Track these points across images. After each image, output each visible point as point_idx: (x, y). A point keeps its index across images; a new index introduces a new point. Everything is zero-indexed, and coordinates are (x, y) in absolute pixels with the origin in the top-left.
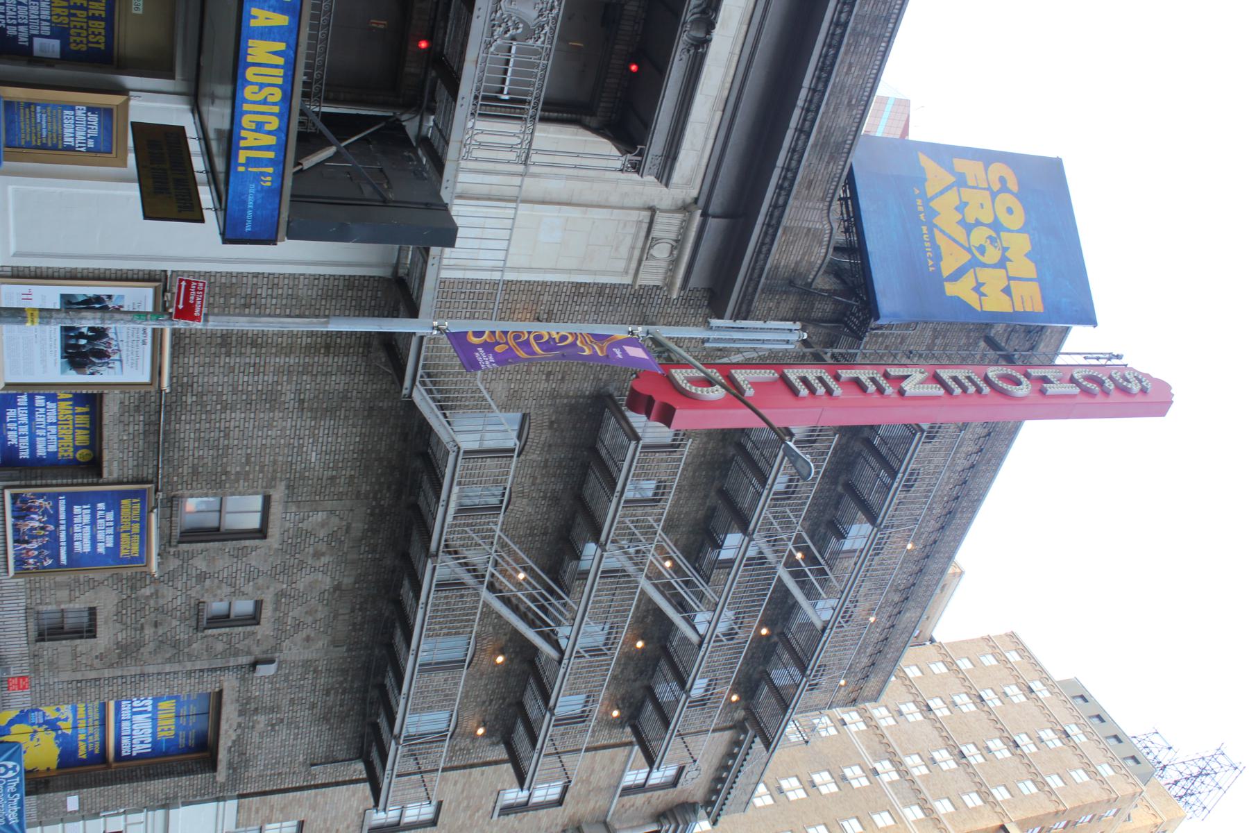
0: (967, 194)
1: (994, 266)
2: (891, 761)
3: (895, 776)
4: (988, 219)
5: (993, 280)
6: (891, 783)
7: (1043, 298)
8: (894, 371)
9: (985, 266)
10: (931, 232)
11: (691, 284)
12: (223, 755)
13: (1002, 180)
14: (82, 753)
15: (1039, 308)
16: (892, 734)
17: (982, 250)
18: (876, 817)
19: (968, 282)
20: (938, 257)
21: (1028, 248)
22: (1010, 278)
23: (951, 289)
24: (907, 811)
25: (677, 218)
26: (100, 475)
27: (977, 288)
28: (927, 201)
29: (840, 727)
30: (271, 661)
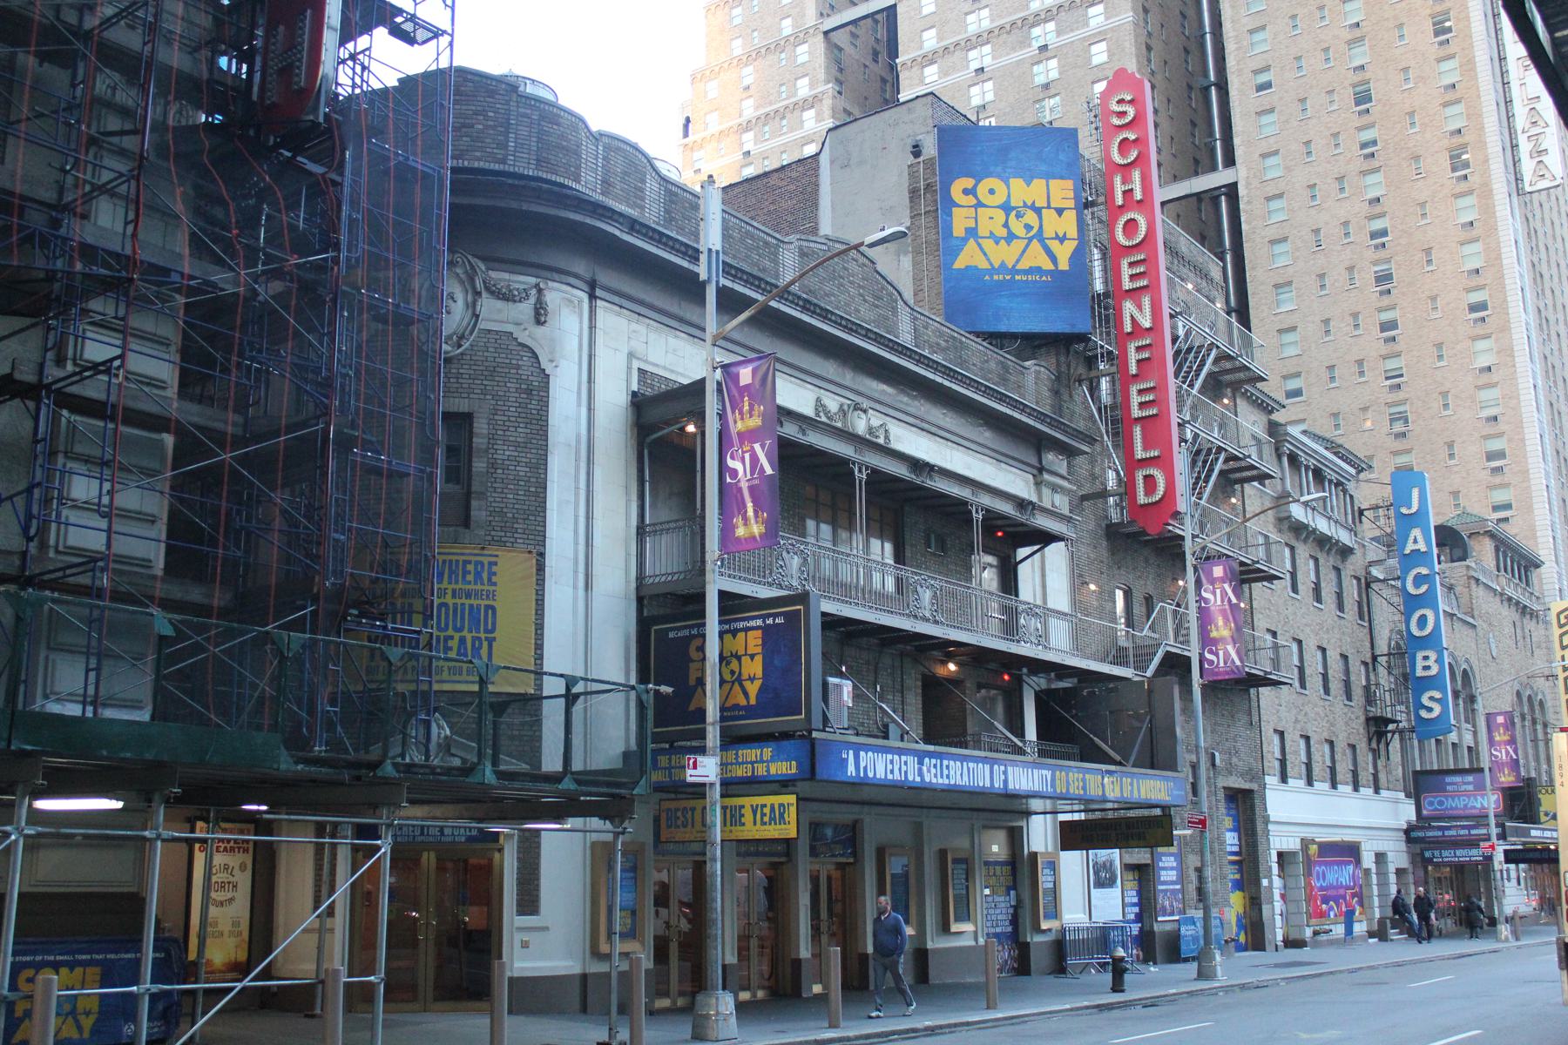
0: (983, 231)
1: (1040, 218)
2: (1033, 26)
3: (1051, 26)
4: (1000, 216)
5: (1052, 225)
6: (1059, 33)
7: (1062, 178)
8: (1128, 328)
9: (1041, 227)
10: (1018, 272)
11: (1063, 470)
12: (1247, 786)
13: (966, 192)
14: (1237, 876)
15: (1069, 184)
16: (1000, 17)
17: (1028, 227)
18: (1096, 61)
19: (1054, 246)
20: (1039, 270)
21: (1020, 181)
22: (1049, 207)
23: (1064, 265)
24: (1093, 23)
25: (1046, 491)
26: (1147, 865)
27: (1062, 239)
28: (992, 270)
29: (985, 76)
30: (1213, 756)
